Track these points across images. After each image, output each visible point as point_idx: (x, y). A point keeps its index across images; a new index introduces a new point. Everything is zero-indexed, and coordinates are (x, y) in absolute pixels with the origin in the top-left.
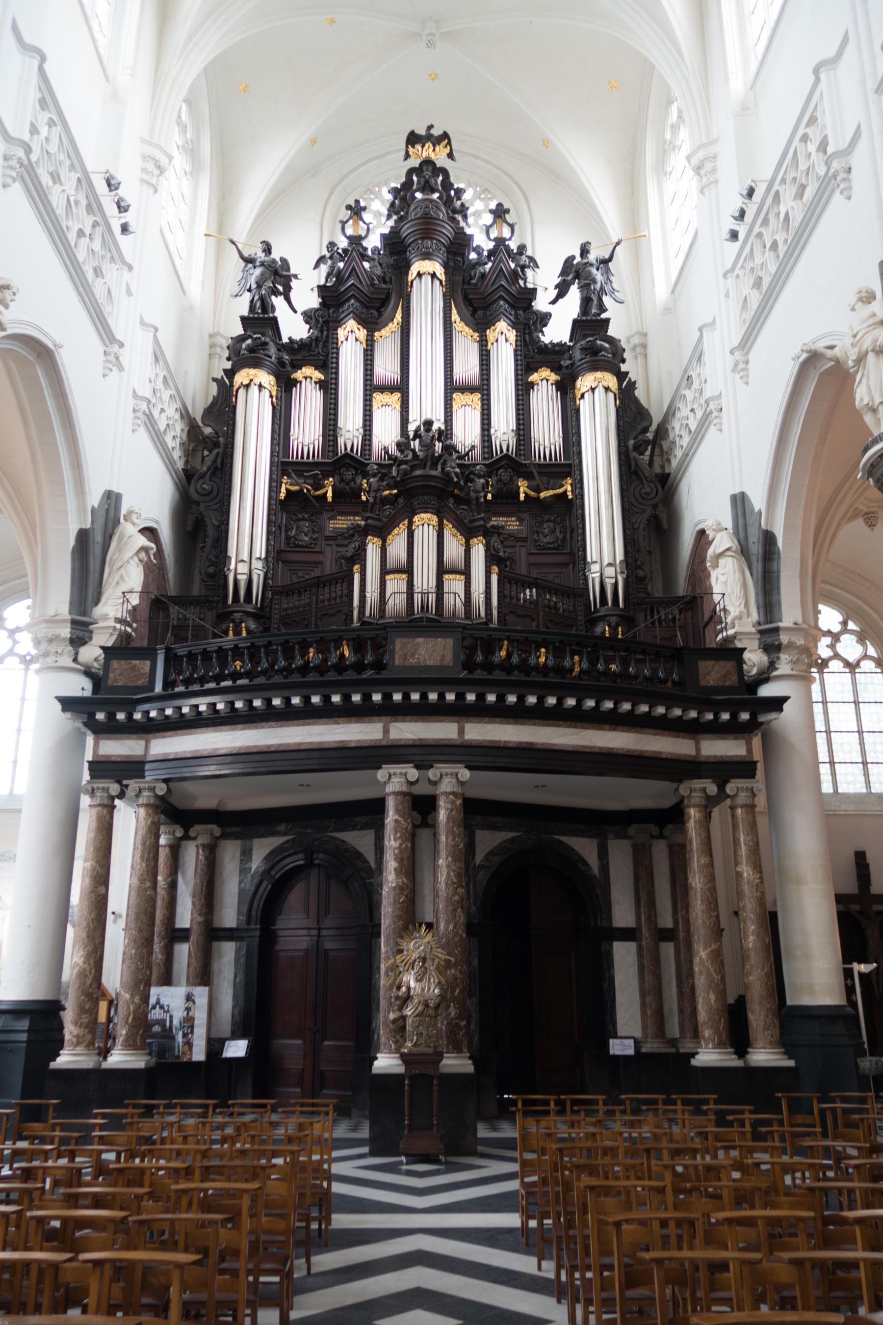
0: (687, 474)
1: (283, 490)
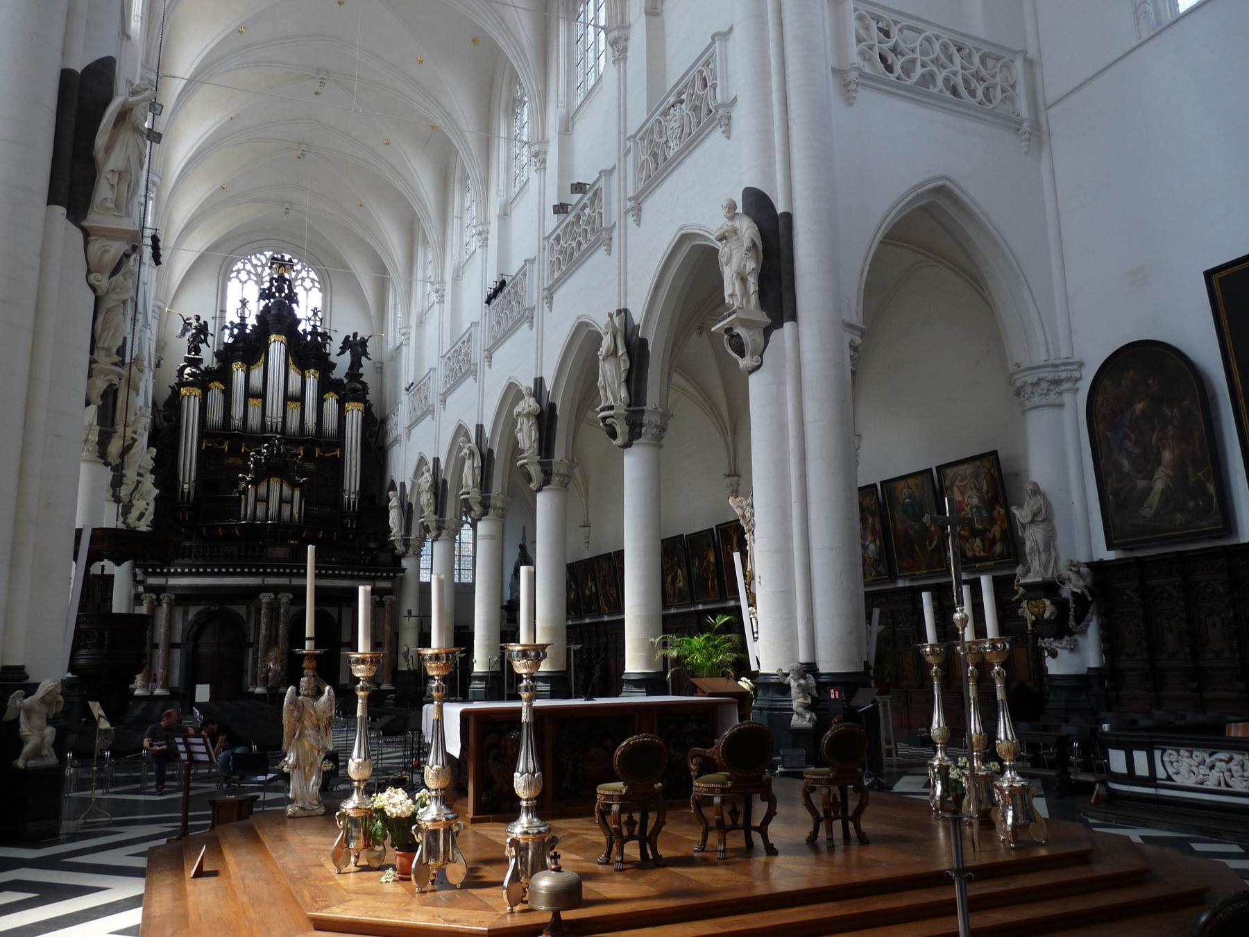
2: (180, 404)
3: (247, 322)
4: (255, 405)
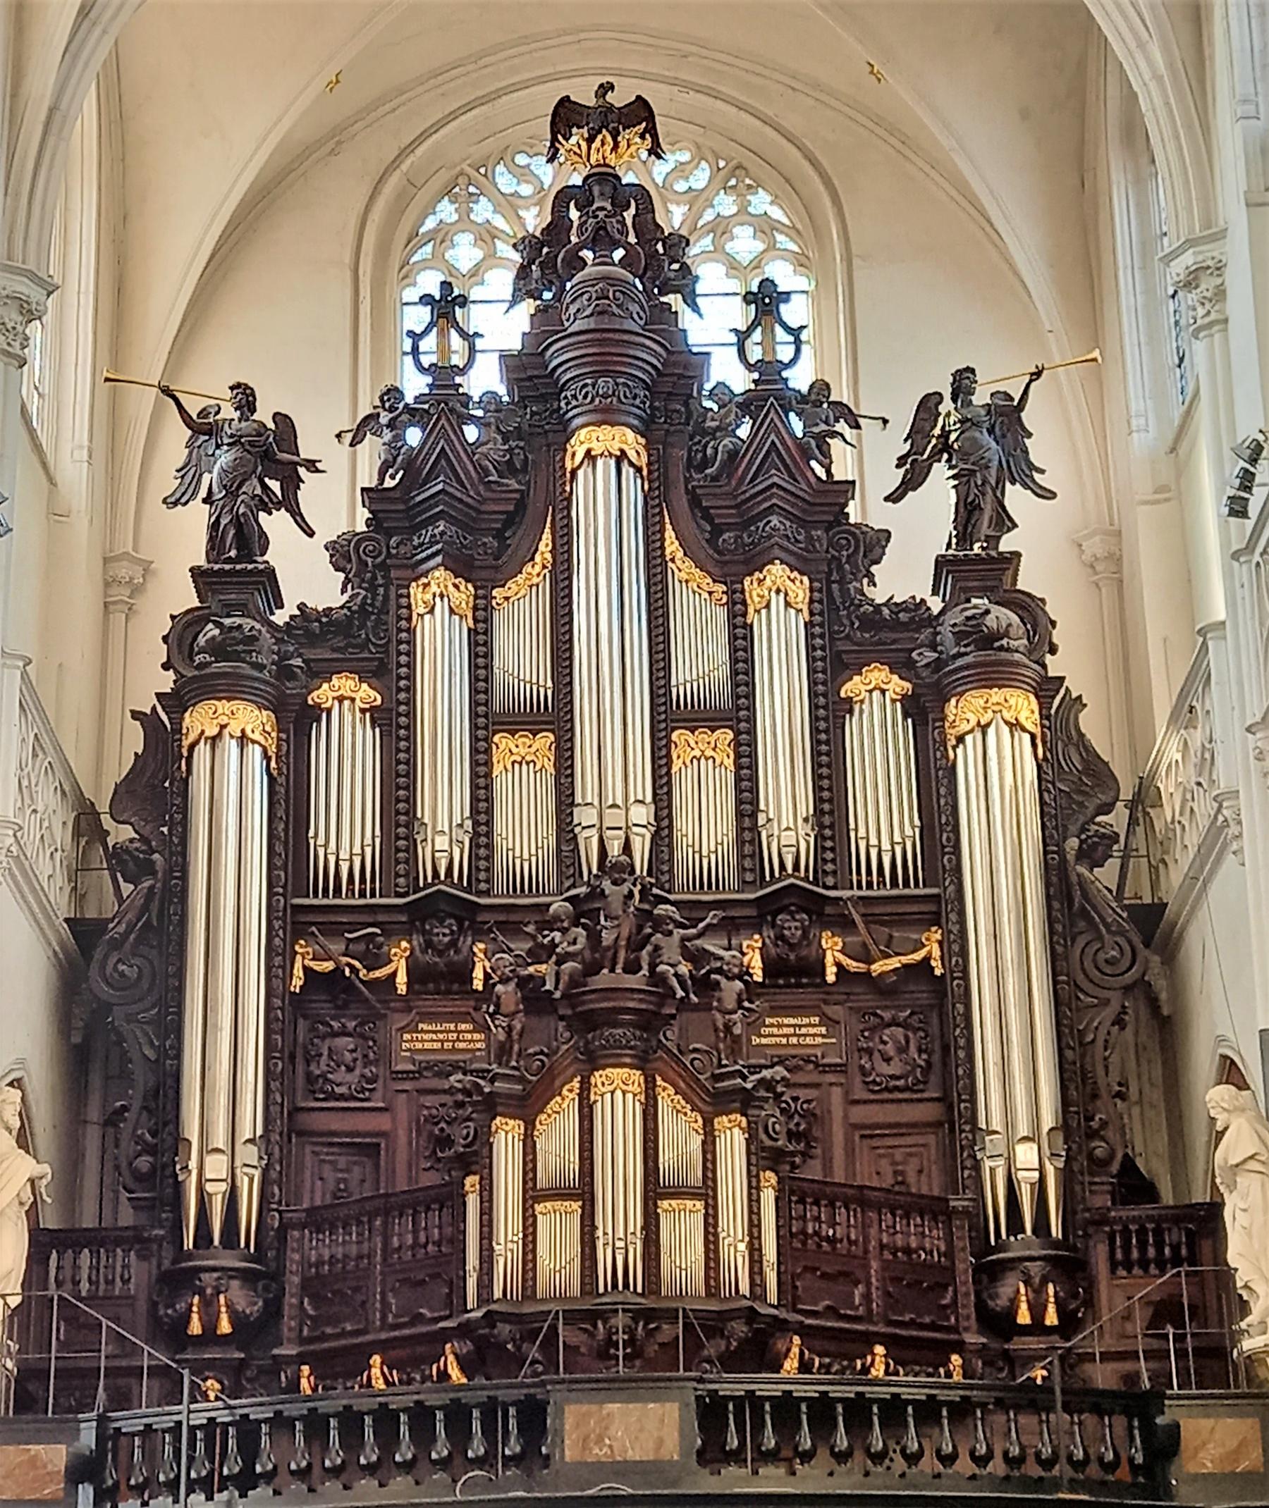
0: (1202, 914)
1: (298, 971)
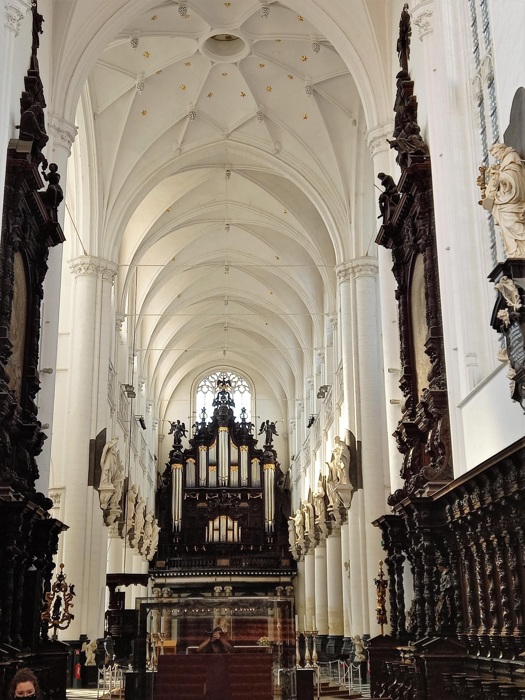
1: (185, 497)
2: (172, 473)
3: (206, 421)
4: (212, 469)
